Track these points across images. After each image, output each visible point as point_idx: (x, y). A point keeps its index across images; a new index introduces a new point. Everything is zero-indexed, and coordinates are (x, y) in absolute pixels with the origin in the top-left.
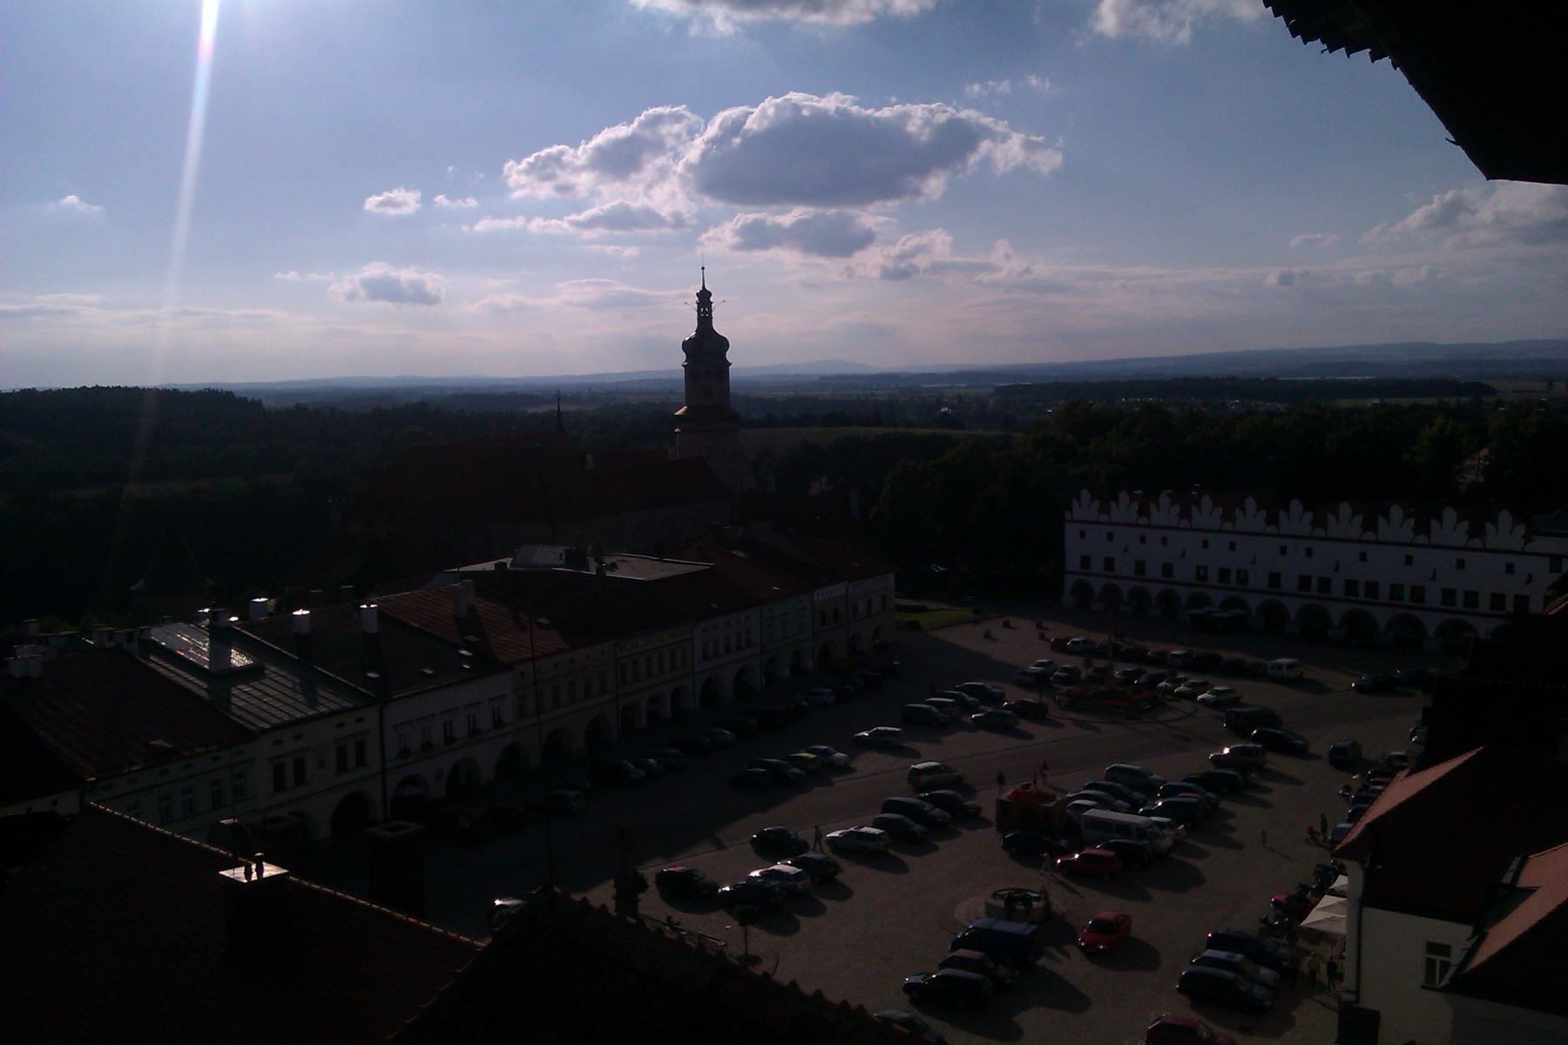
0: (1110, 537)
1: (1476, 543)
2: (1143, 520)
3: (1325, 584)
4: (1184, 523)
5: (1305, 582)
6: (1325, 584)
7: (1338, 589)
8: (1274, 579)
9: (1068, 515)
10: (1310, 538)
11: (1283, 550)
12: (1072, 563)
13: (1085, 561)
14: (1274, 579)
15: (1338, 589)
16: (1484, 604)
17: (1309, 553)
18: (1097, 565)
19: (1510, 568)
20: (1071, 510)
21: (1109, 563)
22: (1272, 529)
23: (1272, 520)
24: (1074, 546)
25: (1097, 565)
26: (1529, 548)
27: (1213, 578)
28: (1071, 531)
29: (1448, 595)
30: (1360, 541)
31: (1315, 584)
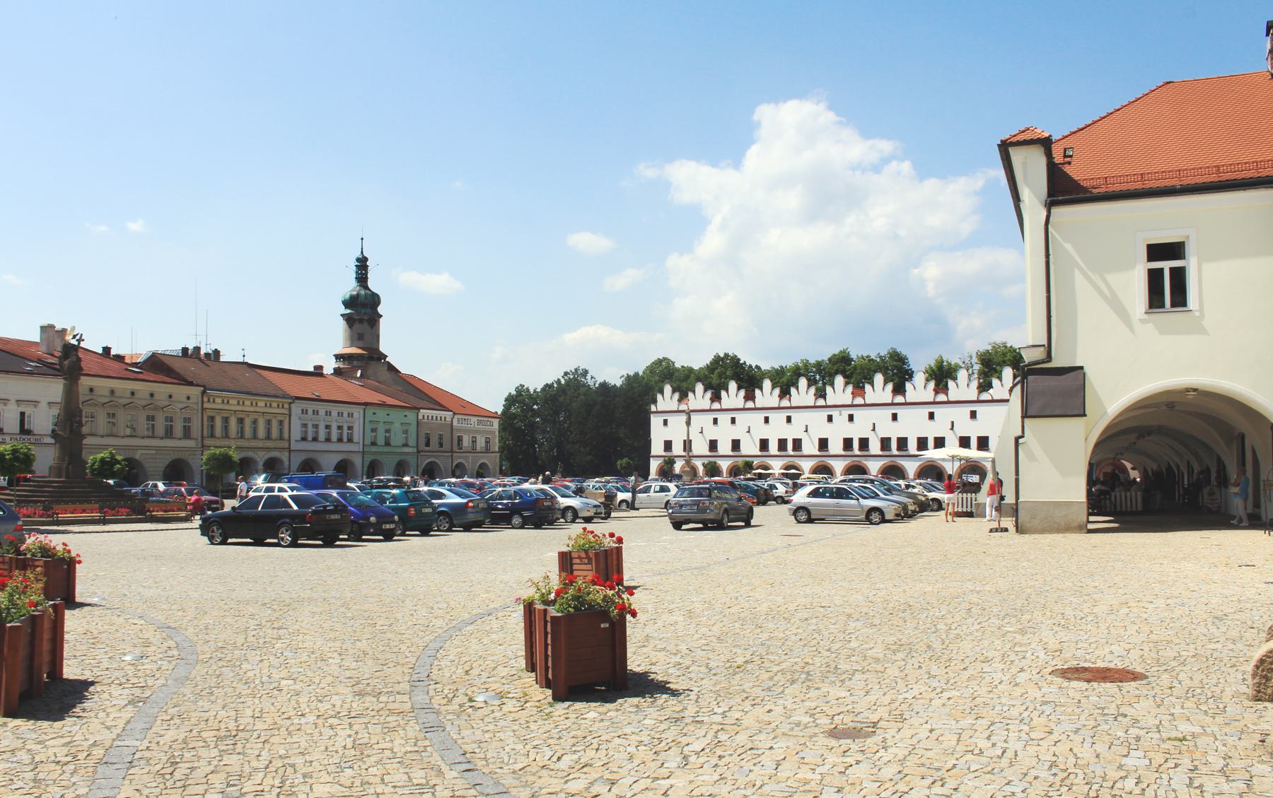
1: (985, 396)
2: (716, 406)
3: (864, 443)
4: (750, 404)
5: (848, 443)
7: (875, 447)
8: (823, 444)
9: (653, 408)
10: (852, 406)
11: (830, 419)
12: (657, 448)
13: (668, 445)
14: (823, 444)
15: (875, 447)
17: (851, 418)
22: (821, 402)
23: (821, 394)
24: (658, 434)
27: (773, 448)
28: (656, 422)
30: (892, 404)
31: (856, 445)
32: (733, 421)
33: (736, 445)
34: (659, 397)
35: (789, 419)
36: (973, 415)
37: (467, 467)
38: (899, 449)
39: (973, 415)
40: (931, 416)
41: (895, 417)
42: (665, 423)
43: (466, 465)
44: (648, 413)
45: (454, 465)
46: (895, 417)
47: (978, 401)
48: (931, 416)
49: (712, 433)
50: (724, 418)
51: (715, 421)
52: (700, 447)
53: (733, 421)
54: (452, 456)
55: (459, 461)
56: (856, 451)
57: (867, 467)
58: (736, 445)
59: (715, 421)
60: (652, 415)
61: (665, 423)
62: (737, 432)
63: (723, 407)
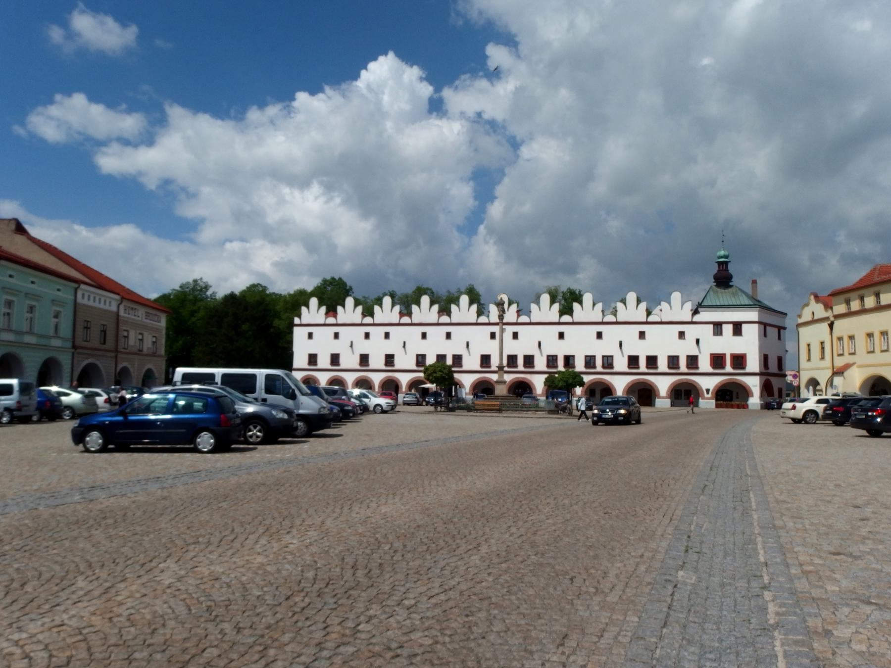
0: (336, 336)
4: (405, 320)
6: (529, 360)
9: (297, 321)
12: (300, 360)
13: (313, 359)
16: (663, 365)
18: (324, 361)
19: (682, 335)
20: (299, 316)
21: (335, 359)
25: (324, 361)
26: (697, 318)
28: (299, 335)
29: (633, 361)
30: (559, 323)
32: (387, 335)
33: (389, 359)
34: (304, 309)
35: (448, 336)
36: (642, 335)
37: (132, 374)
38: (525, 366)
39: (642, 335)
40: (599, 335)
41: (561, 336)
42: (310, 336)
43: (131, 370)
44: (292, 325)
45: (118, 369)
46: (561, 336)
47: (647, 323)
48: (599, 335)
49: (363, 347)
50: (377, 333)
51: (367, 336)
52: (349, 360)
53: (387, 335)
54: (116, 357)
55: (125, 364)
56: (521, 367)
57: (533, 384)
58: (389, 359)
59: (367, 336)
60: (296, 329)
61: (310, 336)
62: (390, 347)
63: (376, 322)
